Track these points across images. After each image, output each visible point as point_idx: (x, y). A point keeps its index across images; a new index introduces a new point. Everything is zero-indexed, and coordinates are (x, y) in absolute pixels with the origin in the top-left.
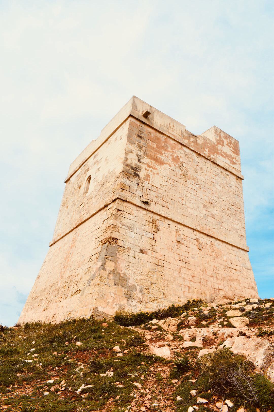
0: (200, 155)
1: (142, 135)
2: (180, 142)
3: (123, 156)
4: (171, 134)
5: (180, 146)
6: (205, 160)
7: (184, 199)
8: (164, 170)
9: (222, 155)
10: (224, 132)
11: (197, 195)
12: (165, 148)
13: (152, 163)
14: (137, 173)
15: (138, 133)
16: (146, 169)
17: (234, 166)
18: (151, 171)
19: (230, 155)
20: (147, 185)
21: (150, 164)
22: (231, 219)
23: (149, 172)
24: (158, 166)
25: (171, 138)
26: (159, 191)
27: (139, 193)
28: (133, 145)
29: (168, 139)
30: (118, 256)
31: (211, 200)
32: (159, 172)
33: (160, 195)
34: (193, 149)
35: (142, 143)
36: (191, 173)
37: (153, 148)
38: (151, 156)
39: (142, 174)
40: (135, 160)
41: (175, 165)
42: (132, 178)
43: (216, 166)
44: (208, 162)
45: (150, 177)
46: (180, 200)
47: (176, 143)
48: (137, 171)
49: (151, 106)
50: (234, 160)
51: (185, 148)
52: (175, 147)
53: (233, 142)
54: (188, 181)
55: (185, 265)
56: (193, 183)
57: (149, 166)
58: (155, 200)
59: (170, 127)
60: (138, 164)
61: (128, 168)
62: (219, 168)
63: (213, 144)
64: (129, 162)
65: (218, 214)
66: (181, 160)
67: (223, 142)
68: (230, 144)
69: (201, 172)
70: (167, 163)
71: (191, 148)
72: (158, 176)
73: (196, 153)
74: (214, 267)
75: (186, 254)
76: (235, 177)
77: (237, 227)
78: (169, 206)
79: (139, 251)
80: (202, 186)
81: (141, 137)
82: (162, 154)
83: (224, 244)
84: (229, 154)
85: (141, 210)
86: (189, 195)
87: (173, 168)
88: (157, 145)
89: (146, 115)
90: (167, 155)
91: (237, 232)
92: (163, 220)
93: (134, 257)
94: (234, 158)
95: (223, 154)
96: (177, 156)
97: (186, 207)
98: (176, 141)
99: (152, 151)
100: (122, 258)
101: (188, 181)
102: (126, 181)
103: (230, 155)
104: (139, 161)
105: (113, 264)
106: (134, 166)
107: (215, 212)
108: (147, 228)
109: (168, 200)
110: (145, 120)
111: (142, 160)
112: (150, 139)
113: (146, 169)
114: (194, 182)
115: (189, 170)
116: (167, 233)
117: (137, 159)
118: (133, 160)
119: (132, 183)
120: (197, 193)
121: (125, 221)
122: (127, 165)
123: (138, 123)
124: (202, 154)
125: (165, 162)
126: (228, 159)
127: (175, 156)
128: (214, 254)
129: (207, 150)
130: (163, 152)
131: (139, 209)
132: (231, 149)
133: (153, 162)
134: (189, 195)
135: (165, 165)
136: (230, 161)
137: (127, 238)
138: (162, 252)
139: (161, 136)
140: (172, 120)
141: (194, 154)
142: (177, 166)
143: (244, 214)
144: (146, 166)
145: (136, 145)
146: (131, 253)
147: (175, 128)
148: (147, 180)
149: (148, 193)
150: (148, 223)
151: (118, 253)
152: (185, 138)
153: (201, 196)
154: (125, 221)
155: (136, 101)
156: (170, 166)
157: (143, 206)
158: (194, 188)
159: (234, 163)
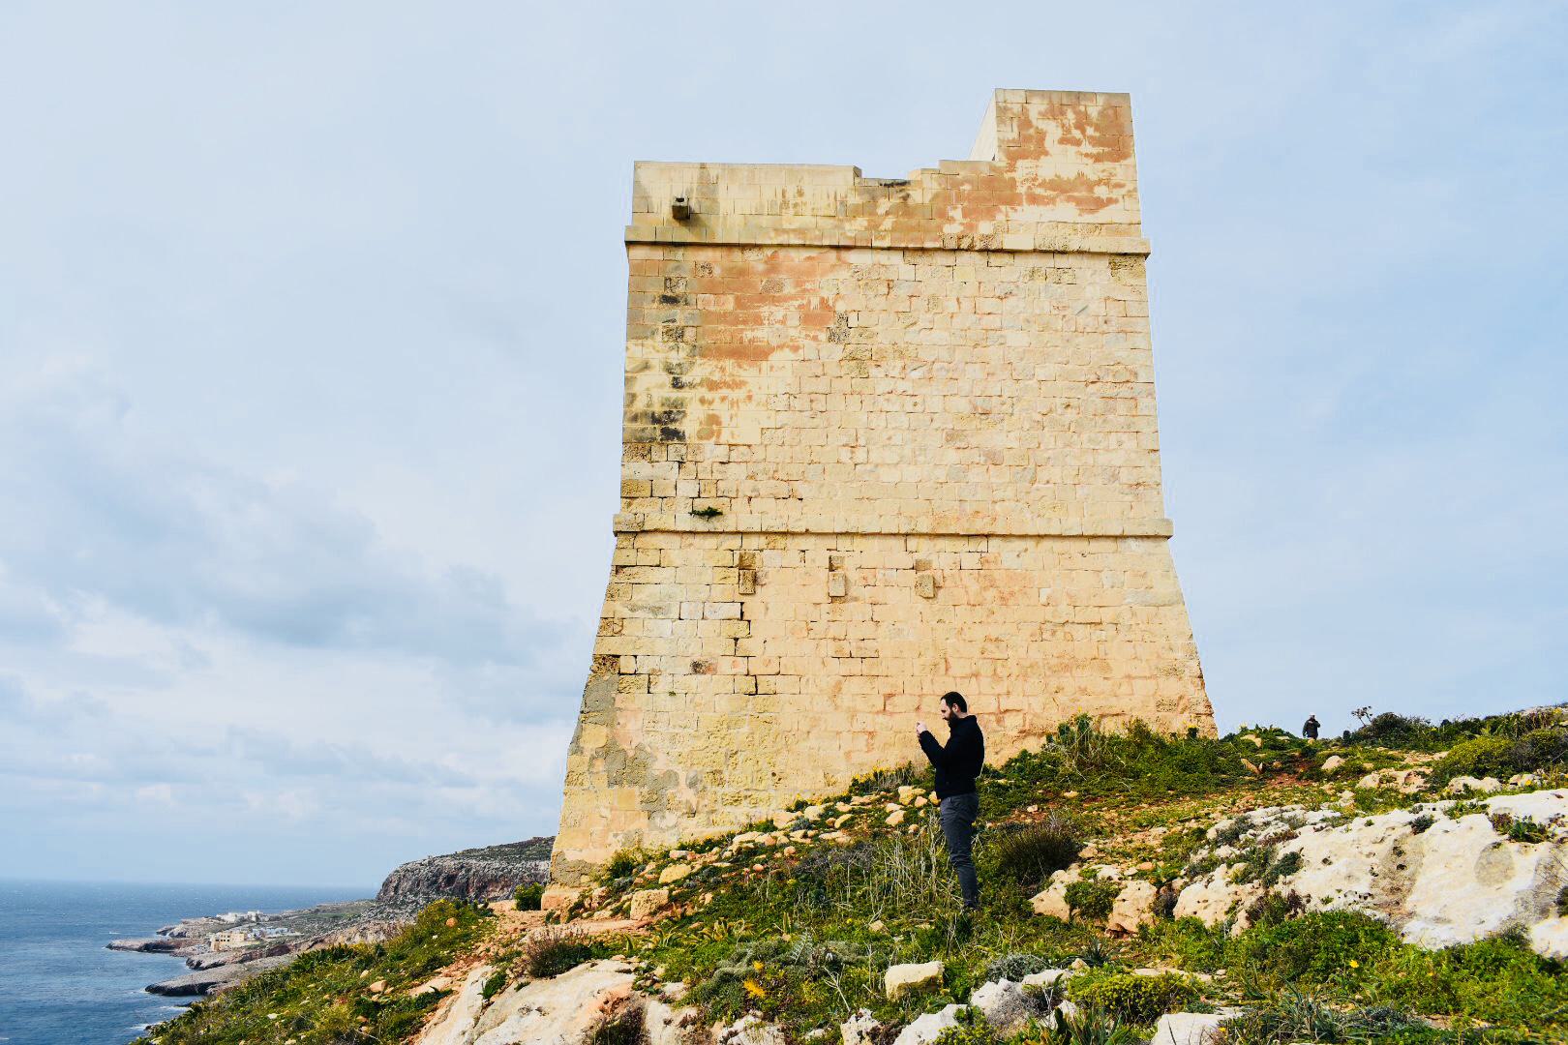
0: (923, 250)
1: (680, 290)
2: (826, 242)
3: (620, 391)
4: (786, 231)
5: (833, 254)
6: (949, 259)
7: (862, 442)
8: (770, 379)
9: (1034, 199)
10: (1042, 94)
11: (919, 408)
12: (770, 295)
13: (723, 369)
14: (672, 426)
15: (662, 292)
16: (702, 401)
17: (1103, 215)
18: (723, 399)
19: (1081, 175)
20: (712, 452)
21: (716, 377)
22: (1085, 437)
23: (717, 405)
24: (747, 373)
26: (760, 454)
27: (688, 489)
28: (649, 342)
29: (782, 253)
30: (618, 704)
31: (979, 402)
32: (755, 391)
33: (761, 466)
34: (886, 244)
35: (680, 314)
36: (886, 333)
37: (722, 317)
38: (718, 349)
39: (688, 426)
40: (662, 386)
41: (815, 338)
42: (657, 452)
43: (1006, 259)
44: (964, 258)
45: (719, 423)
46: (845, 455)
47: (813, 253)
48: (673, 421)
49: (703, 166)
50: (1101, 192)
51: (852, 257)
52: (810, 273)
53: (1093, 112)
54: (873, 371)
55: (855, 666)
56: (895, 373)
57: (713, 386)
58: (747, 488)
59: (785, 204)
60: (675, 394)
61: (638, 425)
62: (1019, 260)
63: (986, 172)
64: (639, 406)
65: (1016, 445)
66: (840, 307)
67: (1041, 136)
68: (1077, 134)
69: (929, 316)
70: (781, 347)
72: (748, 413)
73: (905, 250)
74: (987, 639)
75: (868, 630)
76: (1103, 264)
77: (1117, 458)
78: (801, 489)
79: (690, 670)
80: (936, 366)
81: (671, 300)
82: (758, 321)
83: (1047, 544)
84: (1073, 176)
85: (698, 540)
86: (878, 421)
87: (809, 350)
88: (737, 299)
89: (683, 214)
90: (779, 316)
91: (1115, 477)
92: (781, 542)
93: (672, 694)
94: (1099, 182)
95: (1039, 191)
96: (823, 301)
97: (869, 467)
98: (811, 246)
99: (721, 327)
100: (632, 707)
101: (873, 371)
102: (642, 469)
103: (1081, 175)
104: (677, 384)
105: (604, 730)
106: (658, 409)
108: (717, 590)
109: (795, 471)
110: (683, 234)
111: (684, 379)
112: (713, 289)
113: (702, 401)
114: (899, 364)
115: (875, 329)
116: (792, 583)
117: (668, 379)
118: (655, 390)
119: (661, 468)
120: (917, 399)
121: (643, 596)
122: (635, 418)
123: (658, 254)
124: (927, 245)
125: (774, 342)
126: (1070, 199)
127: (815, 301)
128: (991, 594)
129: (957, 214)
130: (765, 310)
131: (690, 539)
132: (1087, 148)
133: (729, 363)
134: (878, 421)
135: (775, 358)
136: (1079, 202)
137: (655, 642)
138: (772, 650)
139: (752, 256)
140: (793, 171)
141: (896, 258)
142: (823, 336)
143: (1150, 394)
144: (703, 391)
145: (659, 337)
146: (662, 686)
147: (807, 197)
148: (708, 437)
149: (717, 476)
150: (722, 572)
151: (619, 697)
152: (857, 212)
153: (936, 404)
154: (642, 596)
155: (645, 177)
156: (795, 349)
157: (701, 525)
158: (901, 386)
159: (1100, 204)
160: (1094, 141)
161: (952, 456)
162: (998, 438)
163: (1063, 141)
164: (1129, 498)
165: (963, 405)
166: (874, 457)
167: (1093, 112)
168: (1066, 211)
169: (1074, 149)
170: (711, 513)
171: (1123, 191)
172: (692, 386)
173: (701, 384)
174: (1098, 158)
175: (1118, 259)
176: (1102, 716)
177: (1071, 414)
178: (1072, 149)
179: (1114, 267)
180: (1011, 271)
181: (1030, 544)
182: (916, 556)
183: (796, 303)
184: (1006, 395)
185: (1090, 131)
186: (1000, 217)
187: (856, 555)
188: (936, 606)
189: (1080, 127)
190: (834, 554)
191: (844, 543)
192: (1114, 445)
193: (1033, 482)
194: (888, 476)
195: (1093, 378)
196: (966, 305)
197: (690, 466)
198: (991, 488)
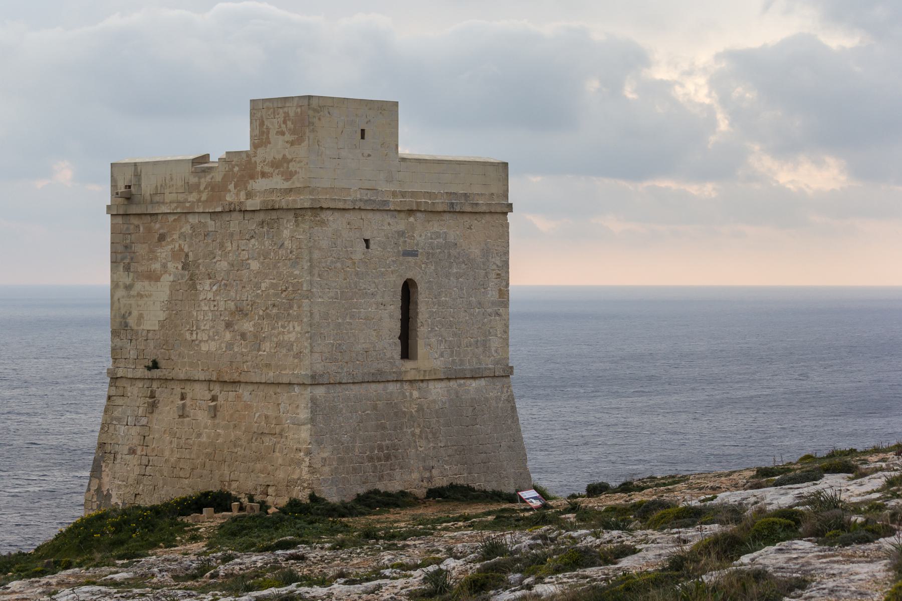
9: (264, 175)
44: (234, 215)
77: (292, 337)
83: (262, 387)
107: (247, 326)
120: (216, 303)
132: (288, 137)
158: (210, 295)
161: (228, 336)
162: (247, 326)
165: (232, 305)
174: (292, 143)
175: (298, 212)
177: (275, 311)
178: (281, 137)
179: (296, 216)
181: (256, 386)
184: (249, 299)
185: (289, 123)
188: (217, 421)
192: (291, 329)
193: (259, 350)
194: (204, 348)
197: (134, 341)
198: (242, 354)
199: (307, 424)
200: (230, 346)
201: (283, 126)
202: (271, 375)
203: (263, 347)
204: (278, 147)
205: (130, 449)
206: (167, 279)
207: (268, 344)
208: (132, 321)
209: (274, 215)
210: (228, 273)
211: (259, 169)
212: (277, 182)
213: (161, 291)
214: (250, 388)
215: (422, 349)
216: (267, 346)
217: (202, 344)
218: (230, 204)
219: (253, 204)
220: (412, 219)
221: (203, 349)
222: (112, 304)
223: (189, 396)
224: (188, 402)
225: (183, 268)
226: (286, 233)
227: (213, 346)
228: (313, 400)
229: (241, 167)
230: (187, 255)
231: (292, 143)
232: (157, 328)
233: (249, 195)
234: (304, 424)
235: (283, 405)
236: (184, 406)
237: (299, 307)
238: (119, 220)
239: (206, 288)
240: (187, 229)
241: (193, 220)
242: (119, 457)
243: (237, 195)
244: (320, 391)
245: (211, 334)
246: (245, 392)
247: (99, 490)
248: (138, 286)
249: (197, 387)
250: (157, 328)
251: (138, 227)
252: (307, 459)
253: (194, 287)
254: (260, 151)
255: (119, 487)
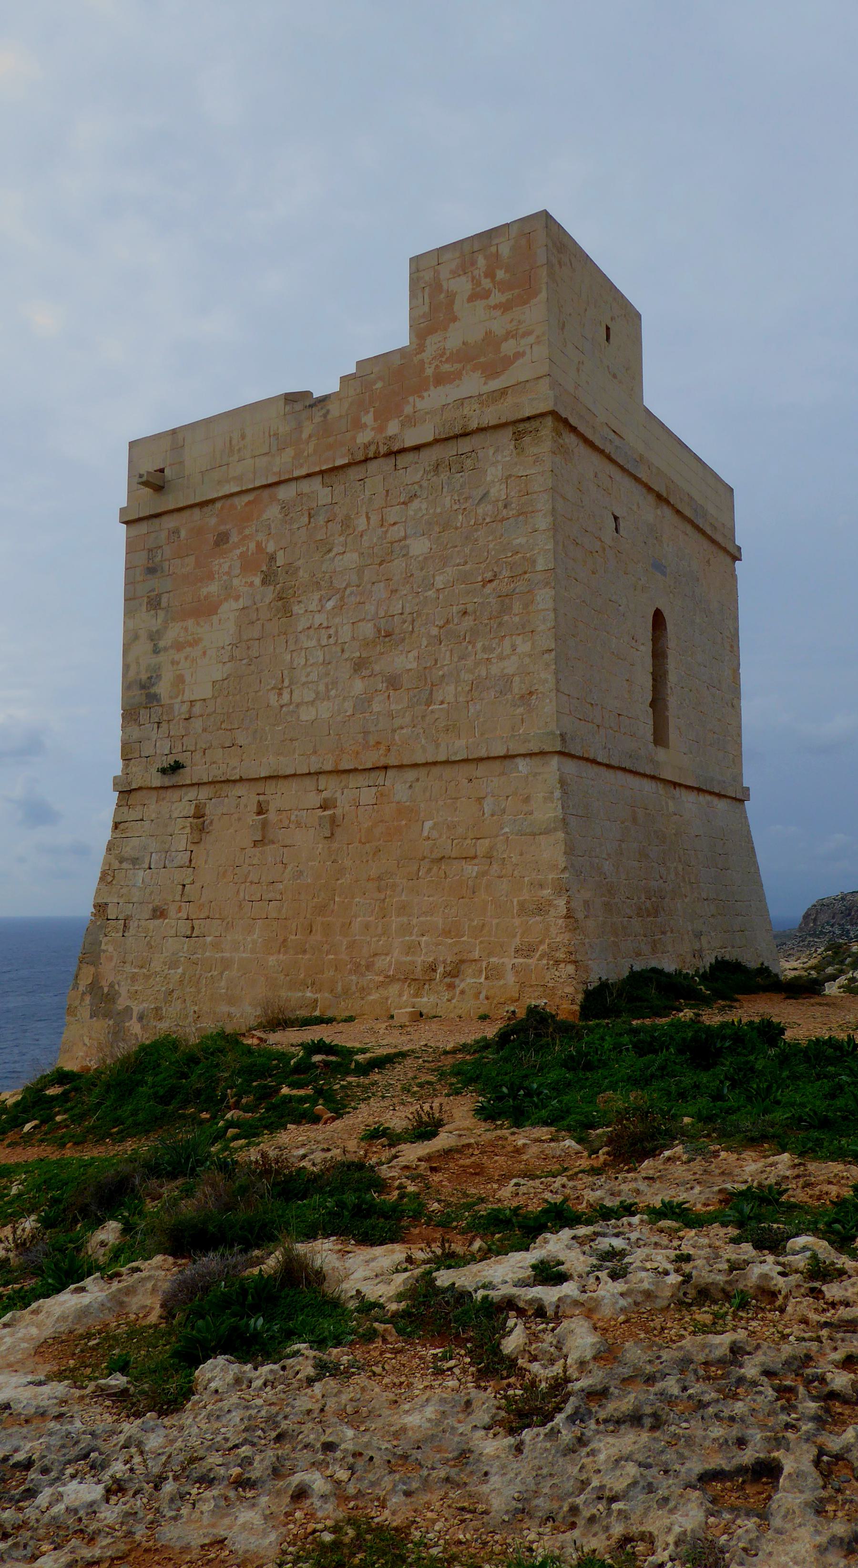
7: (286, 683)
9: (440, 379)
13: (186, 629)
16: (173, 663)
25: (232, 495)
43: (410, 457)
44: (373, 466)
45: (183, 682)
47: (250, 497)
62: (425, 454)
69: (342, 539)
71: (296, 474)
73: (322, 472)
77: (510, 666)
83: (436, 771)
90: (226, 567)
94: (509, 335)
95: (446, 367)
103: (489, 333)
107: (403, 661)
117: (149, 646)
120: (332, 631)
127: (252, 546)
132: (497, 297)
141: (316, 484)
142: (257, 581)
157: (167, 781)
158: (319, 619)
159: (508, 362)
160: (504, 287)
161: (359, 686)
162: (403, 661)
163: (472, 298)
164: (520, 710)
165: (367, 630)
166: (296, 698)
167: (505, 250)
168: (472, 384)
169: (484, 302)
170: (176, 767)
171: (531, 339)
172: (166, 649)
173: (172, 647)
174: (506, 307)
175: (521, 427)
176: (462, 962)
177: (468, 622)
178: (480, 304)
179: (518, 436)
180: (414, 471)
181: (423, 771)
182: (324, 795)
183: (238, 552)
184: (407, 610)
185: (500, 274)
186: (408, 410)
187: (281, 797)
188: (335, 845)
189: (490, 274)
190: (261, 798)
191: (270, 787)
192: (508, 650)
193: (429, 703)
194: (307, 715)
195: (489, 575)
196: (375, 518)
197: (164, 725)
198: (391, 716)
199: (555, 829)
200: (364, 702)
201: (487, 283)
202: (459, 747)
203: (438, 696)
204: (472, 323)
205: (154, 910)
206: (229, 610)
207: (451, 689)
208: (163, 689)
209: (465, 445)
210: (360, 571)
211: (429, 371)
212: (472, 384)
213: (220, 631)
214: (411, 775)
215: (673, 735)
216: (448, 692)
217: (303, 709)
218: (367, 446)
219: (423, 433)
220: (659, 512)
221: (304, 717)
222: (126, 667)
223: (272, 808)
224: (272, 816)
225: (264, 582)
226: (493, 473)
227: (325, 710)
228: (562, 782)
229: (382, 383)
230: (272, 558)
231: (506, 307)
232: (208, 693)
233: (410, 421)
234: (547, 832)
235: (489, 800)
236: (265, 825)
237: (526, 606)
238: (143, 528)
239: (310, 610)
240: (273, 512)
241: (285, 493)
242: (133, 925)
243: (381, 429)
244: (571, 767)
245: (322, 688)
246: (399, 787)
247: (94, 987)
248: (175, 632)
249: (294, 786)
250: (208, 693)
251: (176, 532)
252: (561, 902)
253: (287, 611)
254: (433, 344)
255: (134, 978)
